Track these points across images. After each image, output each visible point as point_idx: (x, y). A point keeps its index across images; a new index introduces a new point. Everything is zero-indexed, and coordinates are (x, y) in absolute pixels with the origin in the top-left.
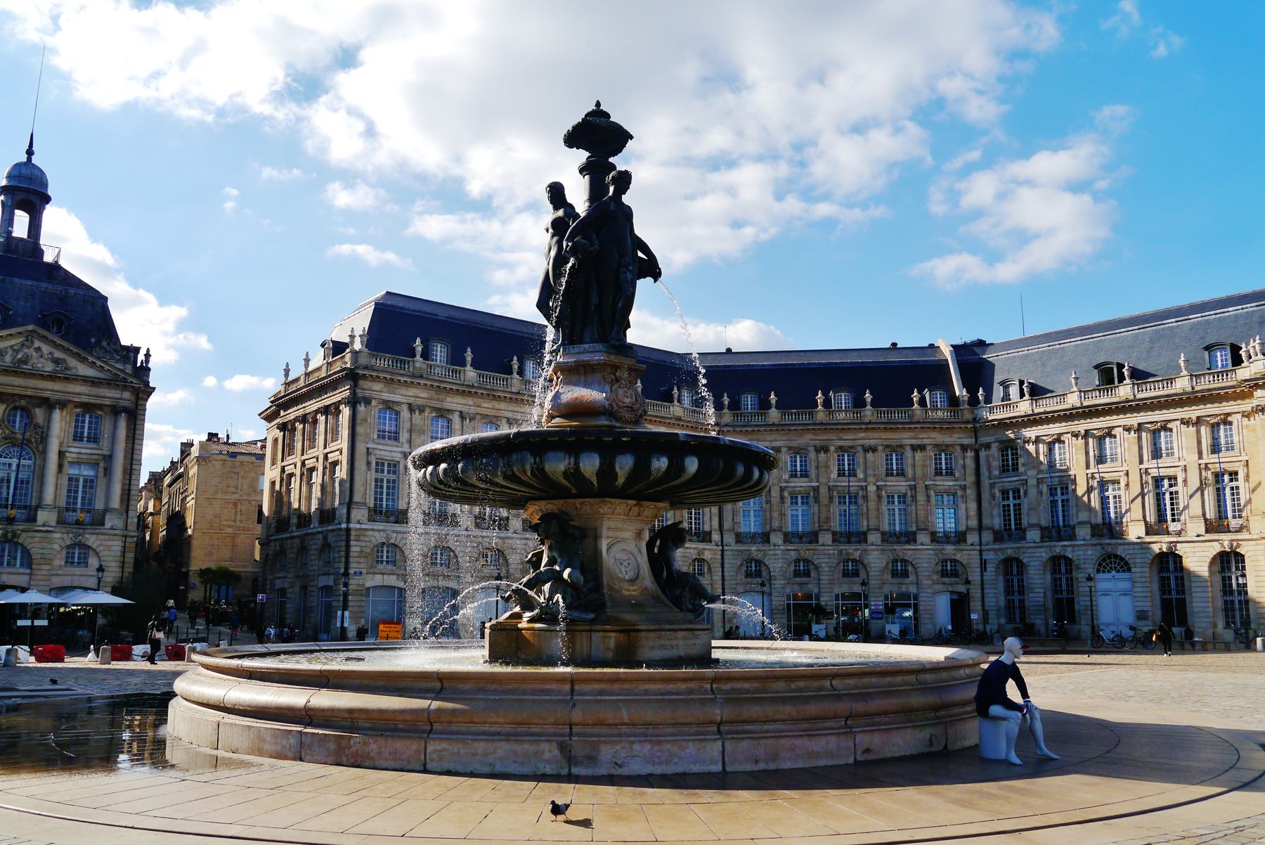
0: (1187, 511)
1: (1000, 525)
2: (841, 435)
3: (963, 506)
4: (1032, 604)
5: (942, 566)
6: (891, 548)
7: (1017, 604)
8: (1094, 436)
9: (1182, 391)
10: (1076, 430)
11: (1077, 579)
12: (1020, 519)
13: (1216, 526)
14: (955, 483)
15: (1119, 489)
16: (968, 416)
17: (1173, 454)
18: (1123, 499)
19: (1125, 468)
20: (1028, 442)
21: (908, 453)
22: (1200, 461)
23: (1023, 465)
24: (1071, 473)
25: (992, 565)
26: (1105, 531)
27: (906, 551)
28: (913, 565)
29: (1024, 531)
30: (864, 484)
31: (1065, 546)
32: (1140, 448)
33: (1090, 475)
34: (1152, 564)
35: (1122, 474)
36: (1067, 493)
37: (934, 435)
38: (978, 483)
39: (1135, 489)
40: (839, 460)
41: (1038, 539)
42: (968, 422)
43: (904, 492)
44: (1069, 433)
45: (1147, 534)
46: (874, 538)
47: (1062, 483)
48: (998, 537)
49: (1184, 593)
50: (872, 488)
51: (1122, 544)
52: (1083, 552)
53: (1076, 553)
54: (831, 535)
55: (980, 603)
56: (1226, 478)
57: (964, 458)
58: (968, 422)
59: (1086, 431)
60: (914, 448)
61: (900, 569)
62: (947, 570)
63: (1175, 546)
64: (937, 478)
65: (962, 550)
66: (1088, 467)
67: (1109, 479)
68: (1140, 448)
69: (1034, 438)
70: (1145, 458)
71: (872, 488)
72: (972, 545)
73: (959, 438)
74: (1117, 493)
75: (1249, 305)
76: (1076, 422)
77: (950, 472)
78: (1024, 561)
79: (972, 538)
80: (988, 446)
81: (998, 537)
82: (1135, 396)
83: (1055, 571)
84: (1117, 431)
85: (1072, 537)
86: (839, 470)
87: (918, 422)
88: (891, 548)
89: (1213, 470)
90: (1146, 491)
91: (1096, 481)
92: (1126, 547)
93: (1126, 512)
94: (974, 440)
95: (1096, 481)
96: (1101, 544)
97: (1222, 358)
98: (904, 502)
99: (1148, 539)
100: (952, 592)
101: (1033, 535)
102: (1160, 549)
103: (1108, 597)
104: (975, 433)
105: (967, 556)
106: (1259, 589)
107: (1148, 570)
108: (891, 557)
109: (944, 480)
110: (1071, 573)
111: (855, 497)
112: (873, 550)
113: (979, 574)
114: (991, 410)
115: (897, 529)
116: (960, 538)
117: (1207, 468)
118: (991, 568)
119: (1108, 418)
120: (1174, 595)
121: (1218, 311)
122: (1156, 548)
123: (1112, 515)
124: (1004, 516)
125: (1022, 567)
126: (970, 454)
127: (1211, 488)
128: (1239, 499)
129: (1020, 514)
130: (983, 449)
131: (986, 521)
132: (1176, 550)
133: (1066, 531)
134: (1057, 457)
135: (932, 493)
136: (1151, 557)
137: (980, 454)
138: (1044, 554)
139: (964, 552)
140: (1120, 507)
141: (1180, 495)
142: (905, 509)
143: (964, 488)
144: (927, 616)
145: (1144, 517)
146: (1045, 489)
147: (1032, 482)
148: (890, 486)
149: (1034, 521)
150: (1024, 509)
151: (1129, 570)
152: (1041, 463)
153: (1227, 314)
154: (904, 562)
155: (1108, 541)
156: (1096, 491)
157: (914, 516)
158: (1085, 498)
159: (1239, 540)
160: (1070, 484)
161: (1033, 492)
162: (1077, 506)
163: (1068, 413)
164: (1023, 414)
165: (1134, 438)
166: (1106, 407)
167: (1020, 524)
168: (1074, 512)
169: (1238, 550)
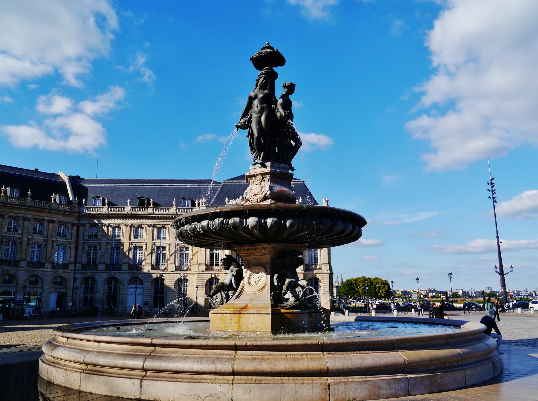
1: (85, 262)
2: (12, 210)
3: (69, 251)
4: (97, 298)
5: (55, 280)
6: (32, 269)
7: (89, 298)
8: (134, 227)
9: (173, 214)
10: (127, 223)
11: (120, 287)
12: (96, 260)
13: (178, 268)
14: (66, 240)
15: (142, 250)
16: (77, 210)
18: (143, 254)
20: (104, 226)
21: (46, 224)
22: (176, 242)
23: (100, 236)
24: (121, 241)
25: (79, 280)
26: (134, 267)
27: (39, 271)
28: (41, 279)
29: (97, 265)
30: (21, 236)
31: (117, 273)
32: (153, 234)
34: (152, 282)
35: (145, 244)
36: (119, 250)
37: (59, 216)
38: (77, 242)
39: (149, 250)
40: (9, 223)
41: (104, 269)
42: (76, 213)
43: (41, 242)
44: (124, 224)
45: (152, 270)
46: (23, 264)
47: (119, 245)
48: (84, 267)
49: (163, 294)
50: (25, 239)
51: (140, 273)
52: (123, 275)
53: (121, 276)
54: (26, 263)
55: (71, 298)
56: (161, 249)
57: (72, 229)
58: (76, 213)
59: (131, 224)
60: (49, 222)
61: (34, 280)
62: (57, 281)
63: (163, 275)
64: (58, 237)
65: (66, 272)
66: (130, 239)
67: (139, 245)
68: (153, 234)
69: (107, 224)
70: (155, 238)
71: (25, 239)
72: (71, 270)
73: (71, 220)
74: (141, 252)
75: (195, 185)
76: (127, 220)
77: (64, 235)
78: (96, 279)
79: (71, 267)
80: (84, 225)
81: (84, 267)
82: (154, 213)
83: (110, 283)
84: (144, 226)
85: (120, 269)
86: (8, 228)
87: (53, 210)
88: (32, 269)
89: (180, 246)
90: (153, 252)
91: (132, 246)
92: (143, 274)
93: (144, 260)
94: (78, 222)
95: (132, 246)
96: (132, 273)
97: (188, 203)
98: (40, 247)
99: (152, 272)
100: (58, 292)
101: (101, 267)
102: (157, 276)
103: (132, 295)
104: (79, 218)
105: (68, 275)
106: (192, 293)
107: (150, 284)
108: (31, 274)
109: (61, 239)
110: (117, 284)
111: (15, 243)
112: (22, 270)
113: (72, 284)
114: (88, 209)
115: (35, 260)
116: (65, 266)
117: (155, 244)
118: (78, 281)
119: (141, 220)
120: (159, 295)
122: (154, 276)
123: (138, 261)
124: (88, 258)
125: (94, 281)
126: (75, 228)
127: (178, 253)
129: (96, 257)
130: (82, 226)
131: (79, 259)
132: (163, 277)
133: (116, 266)
134: (116, 234)
135: (55, 244)
136: (153, 279)
137: (80, 228)
138: (105, 276)
139: (67, 273)
140: (142, 258)
141: (166, 255)
142: (40, 251)
143: (70, 243)
144: (45, 304)
145: (151, 262)
146: (109, 247)
147: (104, 244)
148: (35, 239)
149: (102, 261)
150: (98, 255)
151: (142, 284)
152: (109, 236)
153: (187, 187)
154: (37, 277)
155: (135, 272)
156: (132, 250)
157: (45, 255)
159: (187, 274)
160: (121, 246)
161: (103, 248)
162: (123, 256)
163: (125, 215)
164: (104, 213)
166: (142, 216)
167: (95, 262)
168: (121, 258)
169: (186, 278)
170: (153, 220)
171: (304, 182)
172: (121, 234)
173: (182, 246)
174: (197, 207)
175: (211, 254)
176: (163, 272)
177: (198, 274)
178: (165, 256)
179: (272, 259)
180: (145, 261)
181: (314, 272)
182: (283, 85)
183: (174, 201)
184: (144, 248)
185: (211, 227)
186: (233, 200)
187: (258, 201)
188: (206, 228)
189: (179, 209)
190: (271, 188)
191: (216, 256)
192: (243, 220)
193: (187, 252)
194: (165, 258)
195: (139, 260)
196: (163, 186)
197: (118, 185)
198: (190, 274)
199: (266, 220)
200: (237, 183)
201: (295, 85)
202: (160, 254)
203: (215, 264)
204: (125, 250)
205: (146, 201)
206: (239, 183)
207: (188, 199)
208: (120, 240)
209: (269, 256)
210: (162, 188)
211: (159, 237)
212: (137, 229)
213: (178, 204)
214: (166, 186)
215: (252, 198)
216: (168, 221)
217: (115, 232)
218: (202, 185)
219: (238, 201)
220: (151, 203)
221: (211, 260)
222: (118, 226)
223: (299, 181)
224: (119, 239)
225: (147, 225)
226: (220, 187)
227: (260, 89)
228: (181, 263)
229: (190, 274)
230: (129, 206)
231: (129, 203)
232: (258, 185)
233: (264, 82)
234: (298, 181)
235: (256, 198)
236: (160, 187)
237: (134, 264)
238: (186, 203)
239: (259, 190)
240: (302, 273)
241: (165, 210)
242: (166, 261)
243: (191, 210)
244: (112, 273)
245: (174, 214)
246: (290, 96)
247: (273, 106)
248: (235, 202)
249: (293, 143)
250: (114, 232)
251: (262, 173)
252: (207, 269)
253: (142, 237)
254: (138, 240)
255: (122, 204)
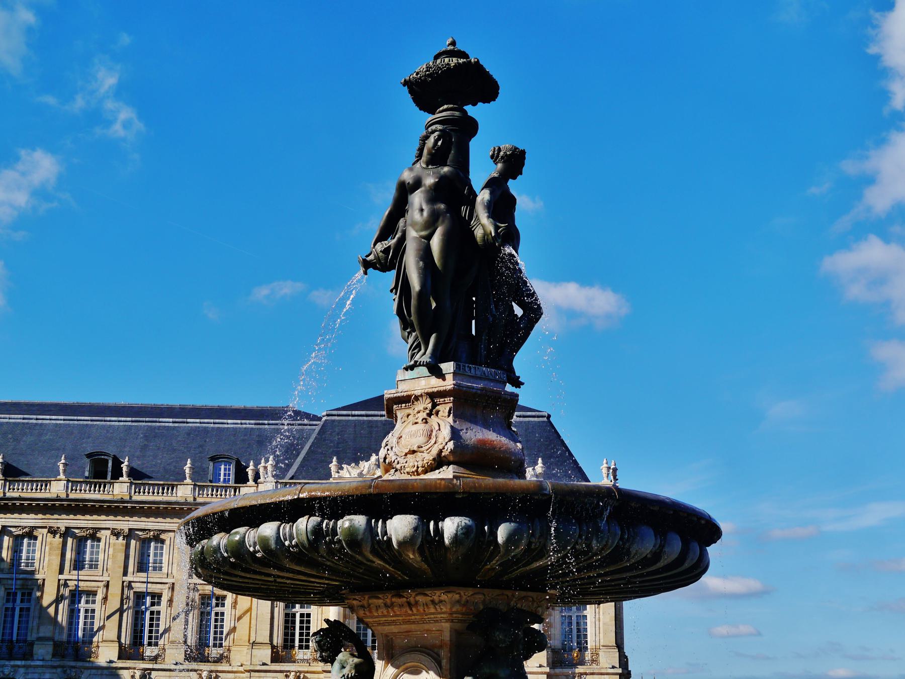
0: (167, 635)
8: (74, 536)
9: (183, 500)
10: (55, 525)
17: (161, 568)
18: (97, 614)
19: (105, 578)
22: (190, 581)
24: (37, 576)
26: (70, 651)
31: (19, 666)
32: (127, 557)
33: (62, 582)
35: (101, 584)
36: (29, 601)
44: (45, 527)
45: (120, 658)
56: (148, 600)
59: (67, 528)
63: (150, 674)
66: (61, 571)
67: (85, 589)
68: (127, 557)
70: (131, 569)
74: (90, 606)
75: (248, 421)
76: (56, 516)
82: (131, 497)
84: (103, 534)
85: (28, 655)
89: (201, 592)
90: (125, 607)
91: (67, 590)
92: (94, 671)
93: (100, 629)
95: (67, 590)
96: (62, 667)
97: (226, 471)
99: (120, 664)
117: (130, 586)
119: (95, 517)
121: (217, 421)
123: (80, 634)
128: (222, 627)
133: (20, 647)
134: (24, 555)
140: (92, 624)
141: (162, 616)
145: (119, 637)
153: (226, 426)
155: (73, 664)
156: (67, 602)
158: (51, 610)
159: (217, 671)
162: (40, 618)
163: (50, 503)
165: (122, 545)
166: (97, 505)
168: (35, 624)
170: (127, 518)
171: (549, 416)
172: (37, 555)
173: (207, 592)
174: (251, 483)
175: (287, 615)
176: (150, 666)
177: (249, 671)
178: (158, 619)
179: (456, 633)
180: (101, 632)
181: (577, 671)
182: (491, 153)
183: (189, 465)
184: (99, 597)
185: (285, 539)
186: (353, 465)
187: (420, 470)
188: (273, 545)
189: (202, 488)
190: (455, 434)
191: (302, 622)
192: (377, 522)
193: (219, 609)
194: (158, 625)
195: (84, 629)
196: (158, 424)
197: (33, 419)
198: (229, 672)
199: (440, 524)
200: (365, 418)
201: (523, 152)
202: (143, 613)
203: (297, 643)
204: (45, 602)
205: (110, 464)
206: (370, 418)
207: (227, 459)
208: (33, 573)
209: (447, 626)
210: (155, 427)
211: (142, 567)
212: (81, 542)
213: (198, 475)
214: (167, 424)
215: (402, 460)
216: (168, 520)
217: (21, 551)
218: (266, 422)
219: (367, 467)
220: (125, 469)
221: (286, 634)
222: (30, 534)
223: (537, 413)
224: (29, 569)
225: (109, 532)
226: (317, 429)
227: (428, 164)
228: (202, 643)
229: (229, 672)
230: (62, 476)
231: (61, 467)
232: (421, 426)
233: (440, 143)
234: (533, 414)
235: (413, 462)
236: (151, 427)
237: (69, 642)
238: (222, 472)
239: (421, 440)
240: (542, 673)
241: (163, 489)
242: (162, 635)
243: (235, 492)
244: (7, 666)
245: (186, 503)
246: (511, 184)
247: (463, 208)
248: (358, 471)
249: (518, 311)
250: (16, 550)
251: (430, 390)
252: (276, 658)
253: (93, 566)
254: (84, 574)
255: (43, 472)
